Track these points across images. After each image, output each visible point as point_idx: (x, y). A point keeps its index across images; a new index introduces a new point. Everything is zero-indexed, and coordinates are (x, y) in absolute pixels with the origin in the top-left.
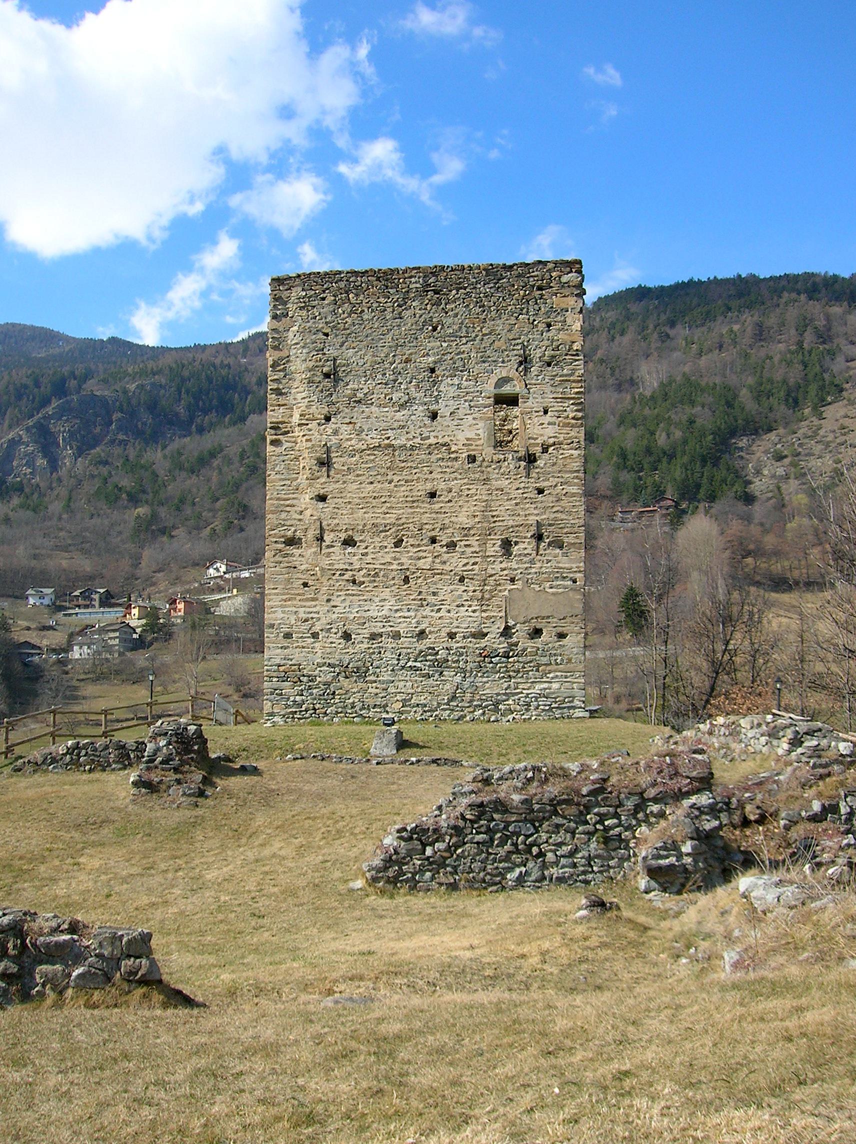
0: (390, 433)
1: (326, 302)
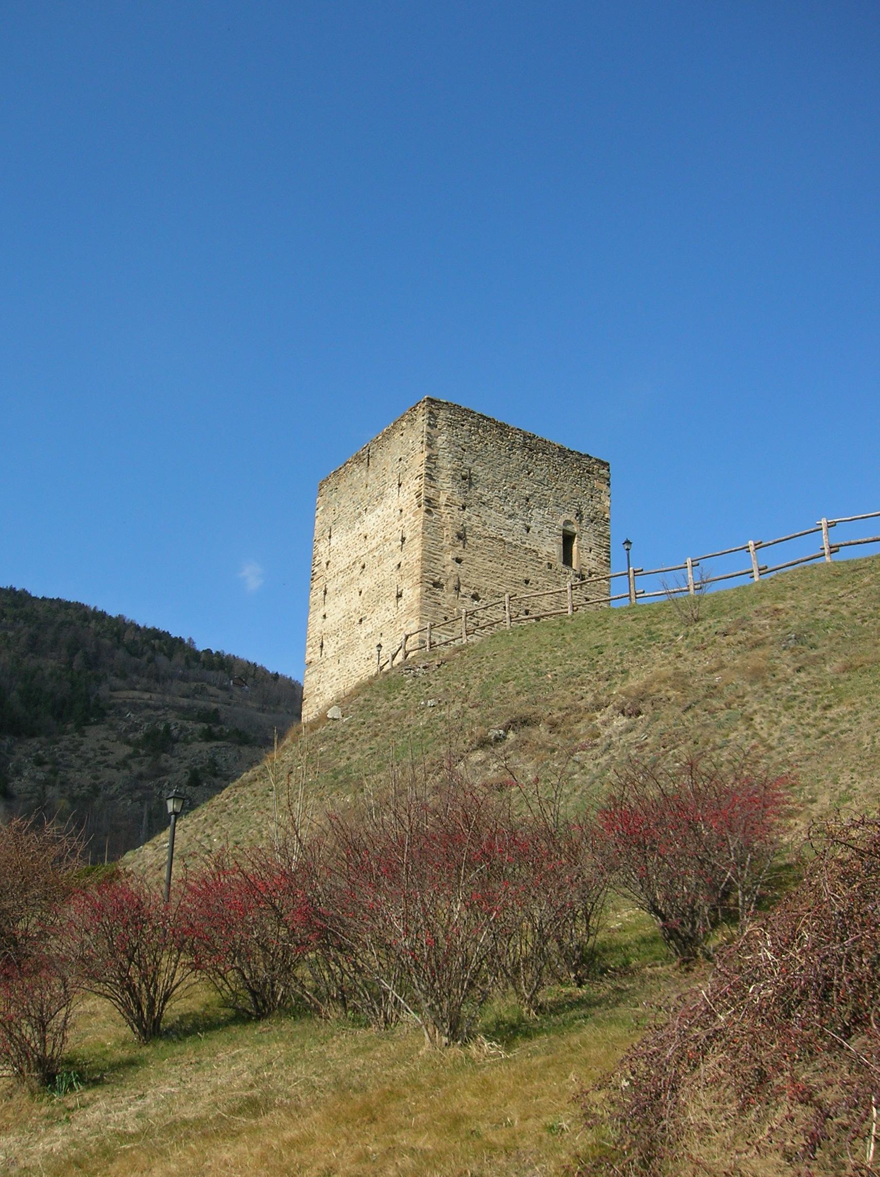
0: (503, 532)
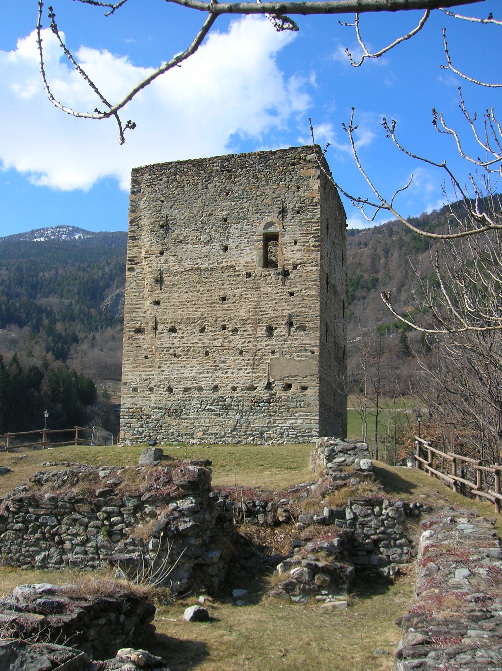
0: (199, 261)
1: (163, 182)
